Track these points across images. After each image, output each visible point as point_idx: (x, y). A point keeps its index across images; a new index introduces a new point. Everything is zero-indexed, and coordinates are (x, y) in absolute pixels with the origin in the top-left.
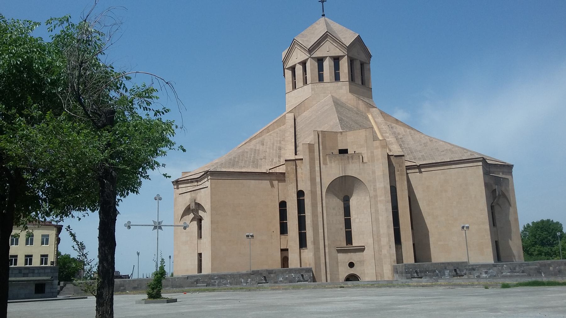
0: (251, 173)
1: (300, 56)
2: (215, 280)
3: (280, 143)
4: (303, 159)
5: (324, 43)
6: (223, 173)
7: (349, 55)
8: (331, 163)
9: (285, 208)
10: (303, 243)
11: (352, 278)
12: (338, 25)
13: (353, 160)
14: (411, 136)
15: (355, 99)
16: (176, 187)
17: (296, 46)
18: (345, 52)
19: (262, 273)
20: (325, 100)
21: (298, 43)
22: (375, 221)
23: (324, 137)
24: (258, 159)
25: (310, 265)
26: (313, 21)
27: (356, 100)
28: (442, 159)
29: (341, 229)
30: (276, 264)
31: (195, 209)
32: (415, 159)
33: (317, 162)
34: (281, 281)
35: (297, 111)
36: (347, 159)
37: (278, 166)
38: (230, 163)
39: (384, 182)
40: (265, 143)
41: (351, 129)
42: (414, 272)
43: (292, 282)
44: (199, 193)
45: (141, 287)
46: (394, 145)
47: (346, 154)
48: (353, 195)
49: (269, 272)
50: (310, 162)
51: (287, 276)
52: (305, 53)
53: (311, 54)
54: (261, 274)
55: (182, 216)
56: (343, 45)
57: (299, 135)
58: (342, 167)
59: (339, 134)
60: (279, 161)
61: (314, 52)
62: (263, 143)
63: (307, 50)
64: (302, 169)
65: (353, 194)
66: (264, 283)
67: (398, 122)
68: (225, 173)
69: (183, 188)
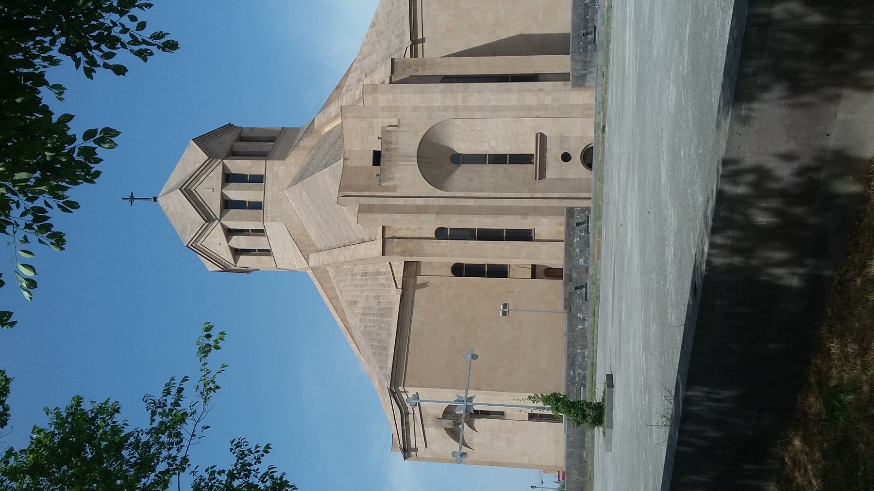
0: (400, 319)
1: (216, 237)
2: (576, 374)
3: (356, 274)
4: (383, 226)
5: (199, 195)
6: (395, 364)
7: (223, 157)
8: (394, 178)
10: (525, 236)
11: (587, 158)
12: (173, 175)
14: (363, 59)
15: (297, 151)
16: (413, 453)
17: (199, 244)
19: (570, 293)
20: (292, 200)
21: (194, 239)
22: (496, 111)
23: (350, 188)
24: (378, 308)
25: (561, 224)
26: (161, 213)
27: (298, 150)
28: (405, 3)
29: (506, 170)
30: (557, 286)
32: (400, 49)
33: (390, 201)
34: (585, 261)
36: (390, 151)
37: (393, 275)
38: (379, 353)
39: (433, 93)
40: (353, 300)
41: (342, 148)
42: (585, 39)
43: (588, 243)
46: (374, 79)
47: (382, 153)
50: (390, 212)
51: (578, 250)
52: (211, 229)
53: (215, 218)
54: (571, 294)
56: (206, 164)
57: (345, 240)
59: (347, 164)
60: (385, 274)
61: (212, 214)
62: (352, 303)
63: (207, 224)
64: (400, 229)
65: (449, 148)
66: (586, 291)
67: (341, 86)
68: (396, 360)
69: (417, 440)
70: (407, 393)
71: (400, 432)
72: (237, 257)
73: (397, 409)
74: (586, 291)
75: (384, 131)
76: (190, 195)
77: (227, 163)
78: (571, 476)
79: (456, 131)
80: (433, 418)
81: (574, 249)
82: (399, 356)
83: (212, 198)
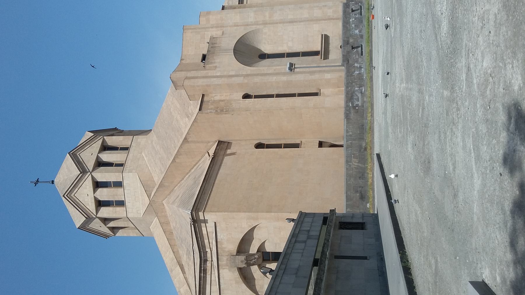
5: (81, 158)
9: (265, 146)
13: (216, 43)
18: (99, 138)
21: (70, 190)
31: (246, 256)
34: (360, 31)
35: (151, 189)
36: (214, 48)
39: (248, 12)
44: (223, 246)
45: (360, 187)
48: (259, 48)
49: (346, 44)
51: (353, 26)
53: (88, 171)
54: (348, 52)
55: (254, 293)
58: (223, 53)
63: (81, 175)
64: (215, 96)
65: (258, 48)
66: (362, 49)
70: (207, 224)
71: (197, 290)
72: (99, 208)
73: (197, 259)
75: (212, 38)
76: (75, 158)
77: (107, 138)
78: (351, 164)
79: (263, 36)
80: (227, 256)
81: (350, 25)
82: (203, 193)
83: (89, 161)
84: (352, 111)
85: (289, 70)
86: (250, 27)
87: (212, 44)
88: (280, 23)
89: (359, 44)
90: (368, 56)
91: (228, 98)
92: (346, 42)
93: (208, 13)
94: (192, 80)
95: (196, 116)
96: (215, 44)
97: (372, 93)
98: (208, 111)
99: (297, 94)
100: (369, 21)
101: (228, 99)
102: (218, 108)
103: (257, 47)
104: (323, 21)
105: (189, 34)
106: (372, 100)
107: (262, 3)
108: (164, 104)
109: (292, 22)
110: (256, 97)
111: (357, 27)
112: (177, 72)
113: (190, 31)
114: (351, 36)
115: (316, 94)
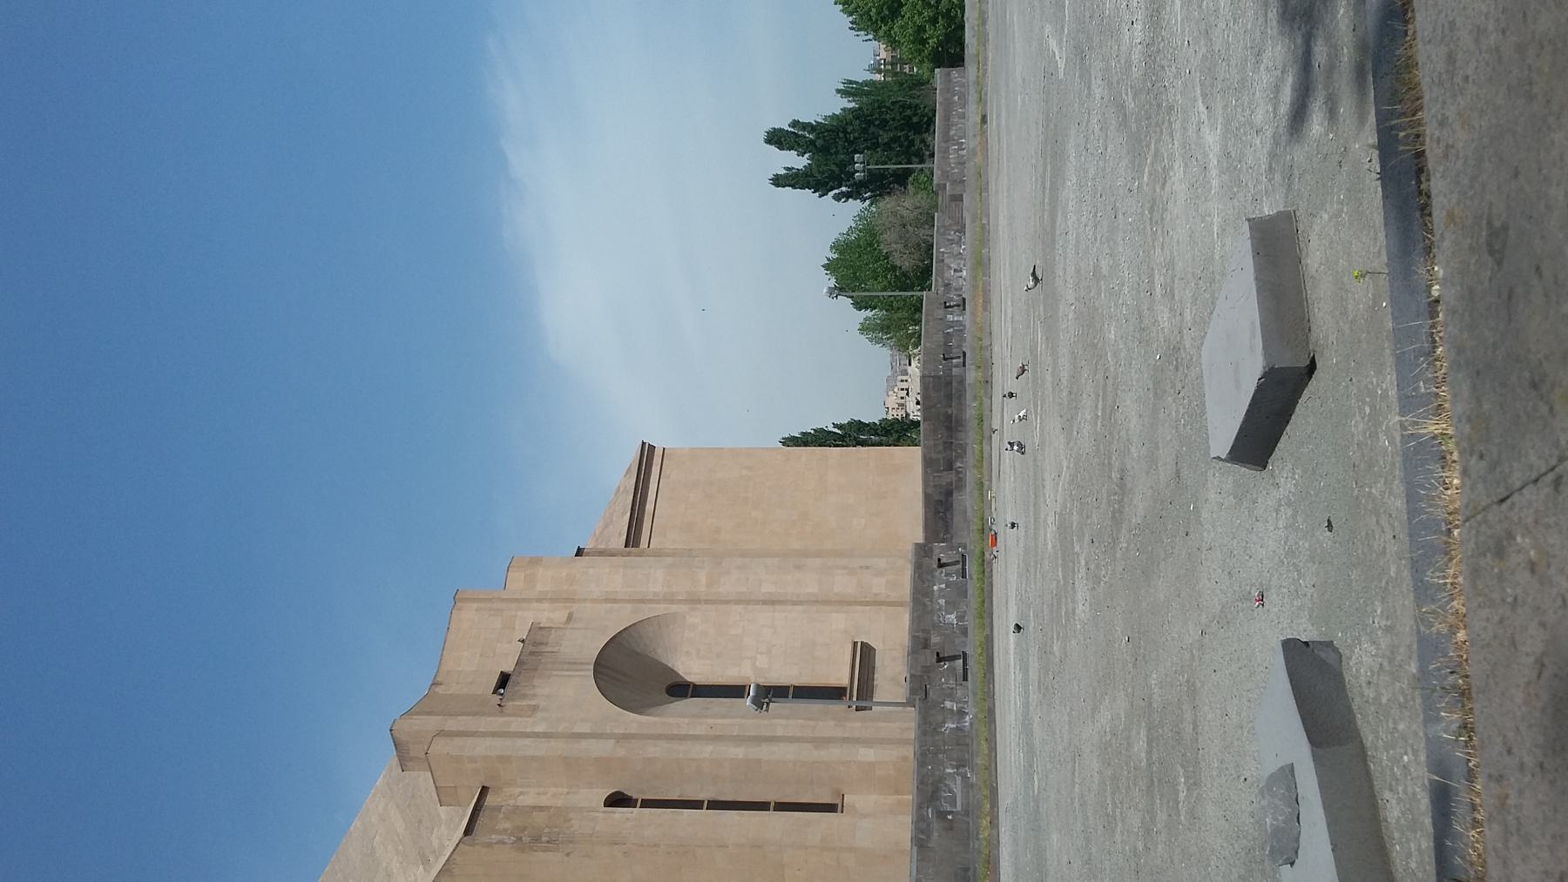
13: (547, 644)
34: (960, 618)
39: (650, 567)
51: (942, 602)
54: (927, 670)
58: (562, 670)
64: (521, 793)
66: (965, 663)
74: (965, 663)
75: (536, 628)
84: (936, 825)
85: (753, 703)
86: (649, 606)
87: (535, 644)
88: (738, 602)
89: (959, 651)
90: (980, 655)
91: (560, 803)
92: (920, 643)
93: (535, 561)
94: (457, 741)
95: (452, 853)
96: (542, 644)
97: (993, 758)
98: (493, 837)
99: (772, 805)
100: (983, 561)
101: (559, 805)
102: (525, 829)
103: (666, 663)
104: (859, 607)
105: (468, 615)
106: (994, 778)
107: (690, 550)
108: (357, 823)
109: (771, 602)
110: (647, 804)
111: (952, 605)
112: (415, 717)
113: (475, 605)
114: (936, 627)
115: (830, 808)
